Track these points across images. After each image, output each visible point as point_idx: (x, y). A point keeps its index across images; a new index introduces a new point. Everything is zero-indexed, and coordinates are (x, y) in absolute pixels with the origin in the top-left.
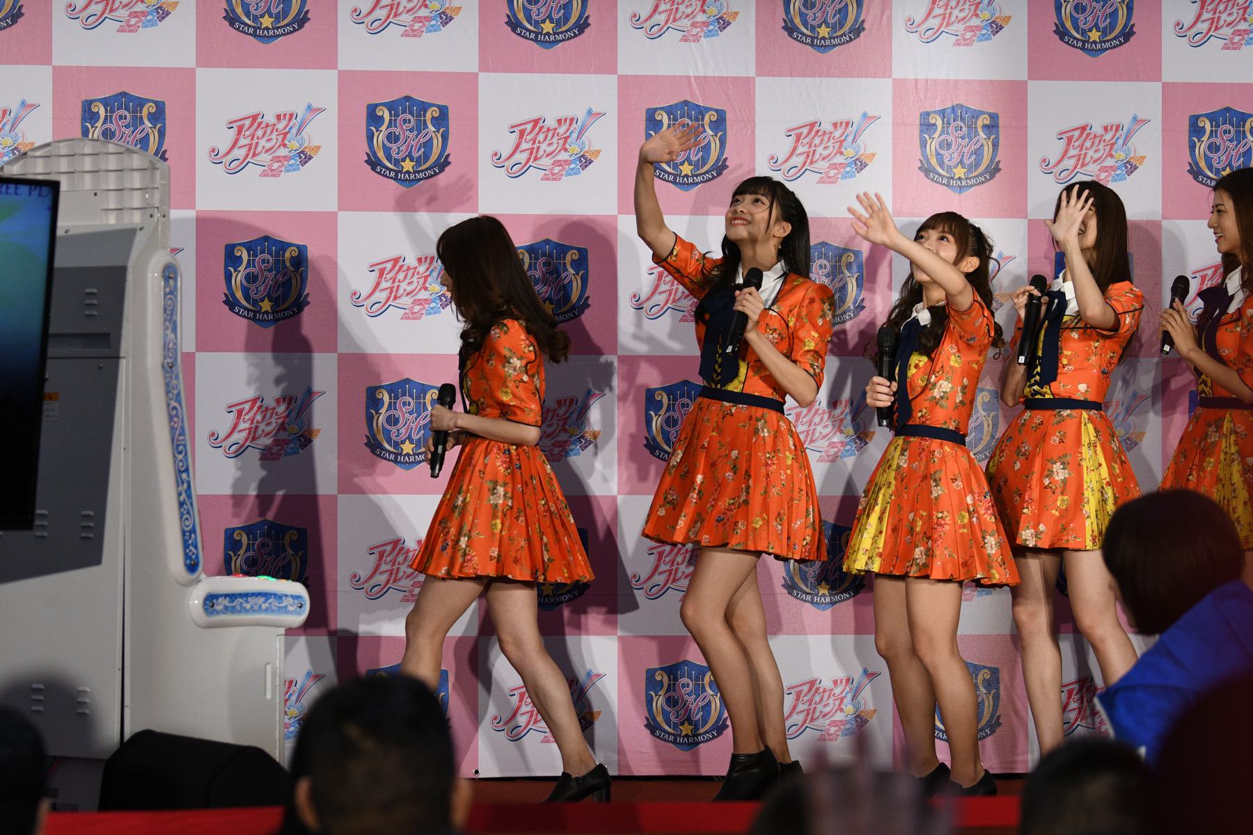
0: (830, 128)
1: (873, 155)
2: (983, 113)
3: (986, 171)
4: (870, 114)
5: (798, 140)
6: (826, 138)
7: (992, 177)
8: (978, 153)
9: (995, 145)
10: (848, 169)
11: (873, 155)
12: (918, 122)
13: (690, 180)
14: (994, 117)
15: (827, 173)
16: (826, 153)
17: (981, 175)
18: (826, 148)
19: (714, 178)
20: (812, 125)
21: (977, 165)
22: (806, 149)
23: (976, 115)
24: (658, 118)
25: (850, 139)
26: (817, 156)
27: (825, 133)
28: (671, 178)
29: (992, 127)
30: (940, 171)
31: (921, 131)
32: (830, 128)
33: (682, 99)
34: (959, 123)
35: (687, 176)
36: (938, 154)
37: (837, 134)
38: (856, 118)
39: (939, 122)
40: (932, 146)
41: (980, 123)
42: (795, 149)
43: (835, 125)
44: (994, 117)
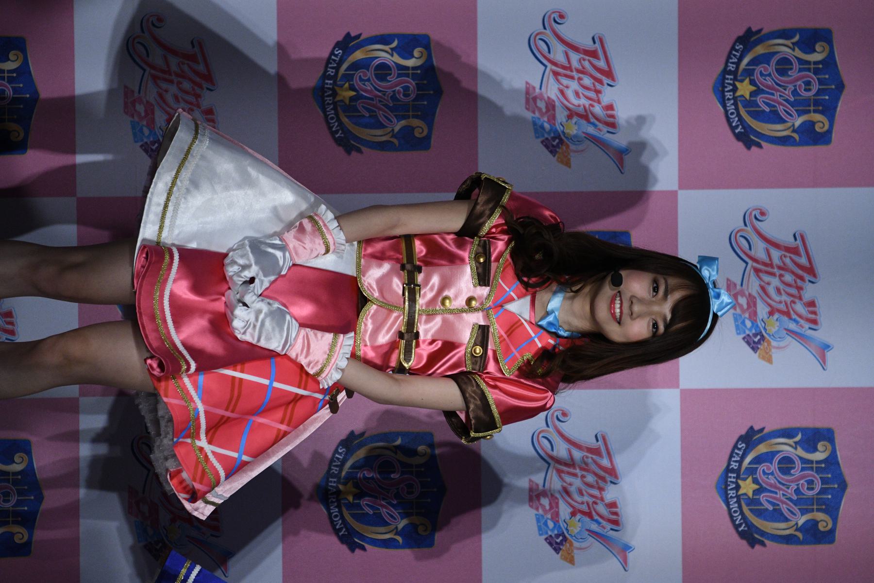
0: (807, 295)
1: (769, 360)
2: (835, 520)
3: (750, 525)
4: (829, 355)
5: (788, 249)
6: (794, 291)
7: (742, 535)
8: (777, 515)
9: (788, 539)
10: (748, 324)
11: (769, 360)
12: (819, 425)
13: (729, 95)
14: (828, 537)
15: (743, 295)
16: (771, 290)
17: (744, 517)
18: (778, 290)
19: (733, 129)
20: (811, 270)
21: (761, 513)
22: (776, 261)
23: (832, 510)
24: (818, 47)
25: (792, 326)
26: (766, 278)
27: (800, 289)
28: (732, 67)
29: (813, 534)
30: (748, 459)
31: (803, 430)
32: (807, 295)
33: (846, 82)
34: (818, 486)
35: (735, 89)
36: (773, 454)
37: (799, 307)
38: (821, 335)
39: (819, 456)
40: (785, 447)
41: (820, 516)
42: (777, 246)
43: (812, 304)
44: (828, 537)
